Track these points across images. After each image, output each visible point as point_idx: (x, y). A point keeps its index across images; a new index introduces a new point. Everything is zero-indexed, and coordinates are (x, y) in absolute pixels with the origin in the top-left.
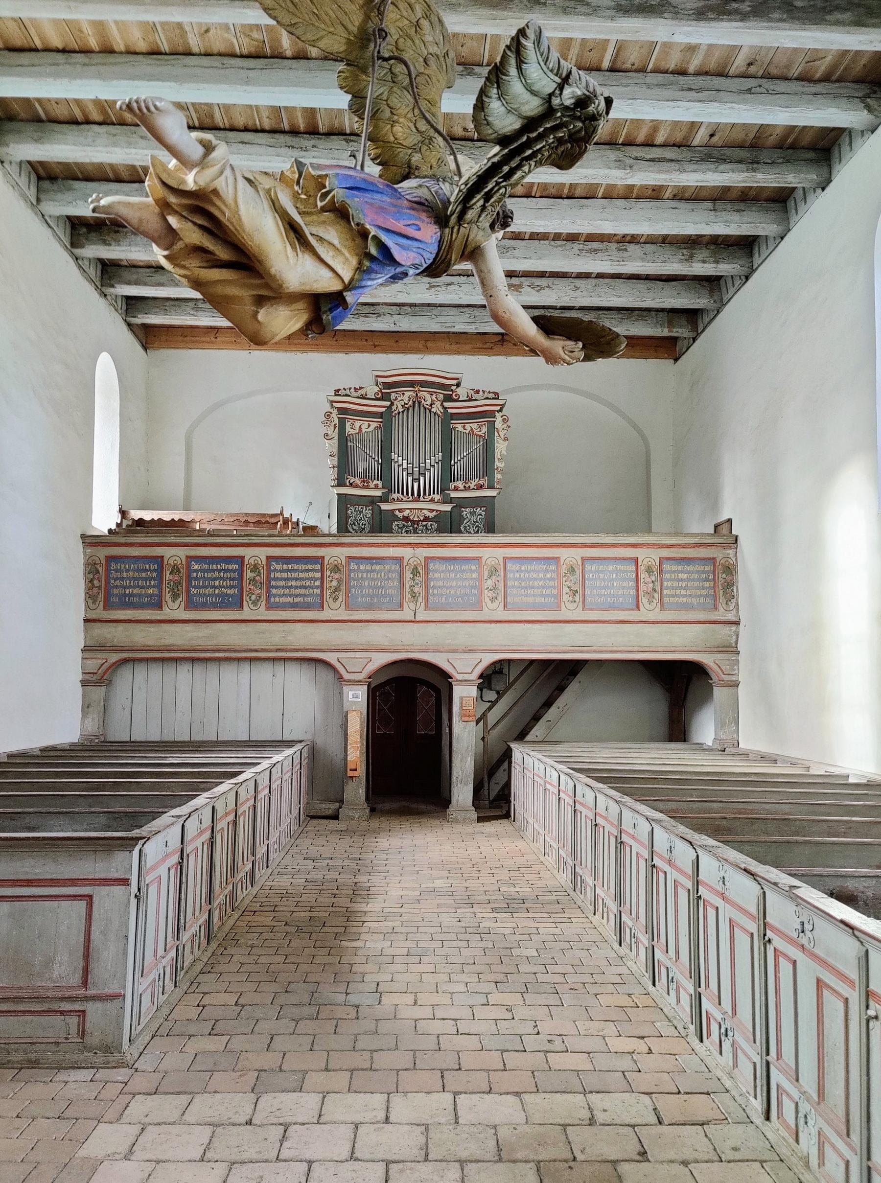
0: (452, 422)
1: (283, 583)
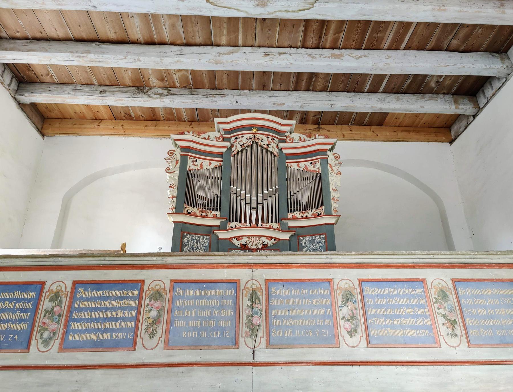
0: (287, 161)
1: (88, 315)
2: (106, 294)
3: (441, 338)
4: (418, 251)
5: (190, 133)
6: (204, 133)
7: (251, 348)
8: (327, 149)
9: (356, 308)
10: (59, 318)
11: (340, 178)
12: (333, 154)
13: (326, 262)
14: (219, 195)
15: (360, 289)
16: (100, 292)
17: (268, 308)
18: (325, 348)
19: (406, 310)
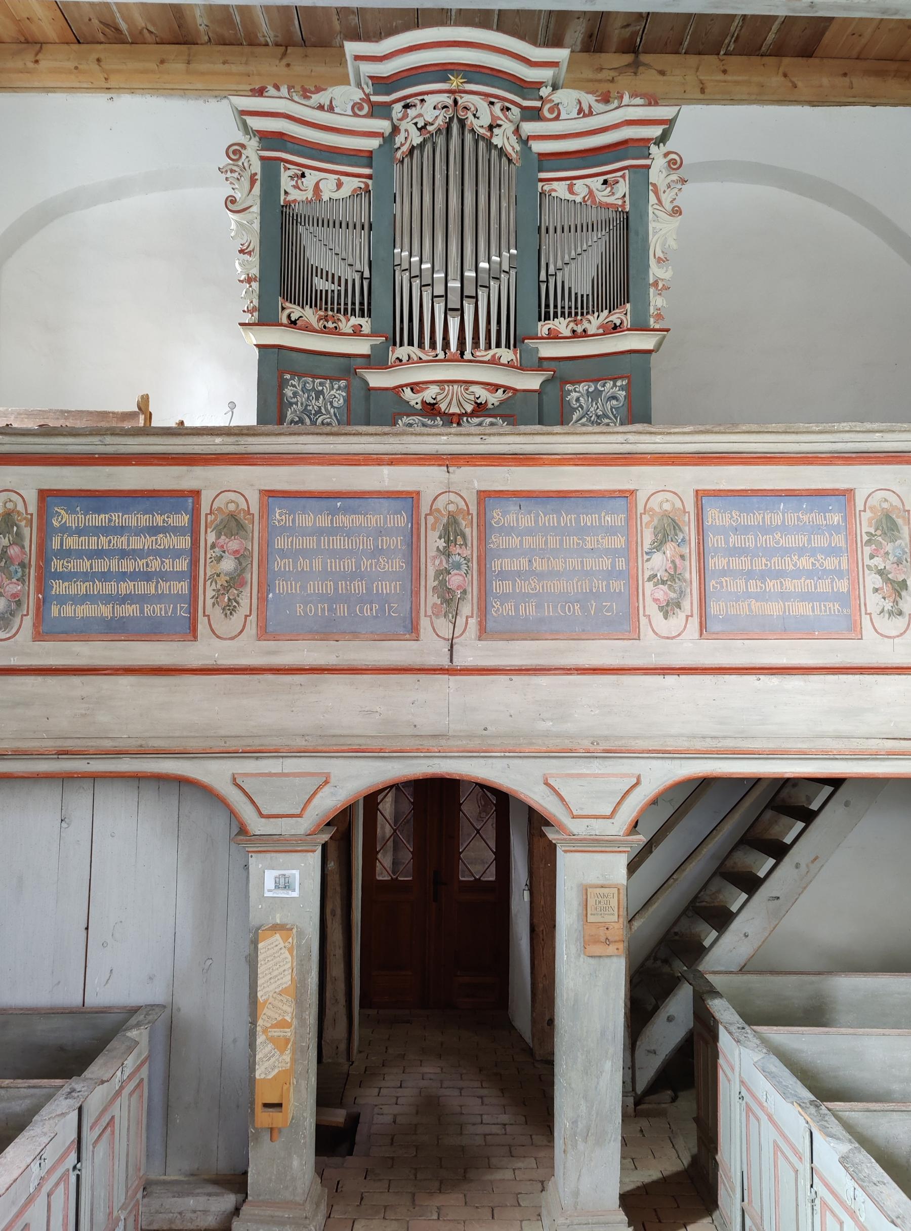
1: (85, 565)
2: (117, 521)
3: (866, 620)
4: (845, 424)
5: (282, 89)
6: (318, 90)
7: (445, 639)
8: (648, 140)
9: (682, 557)
10: (23, 571)
11: (677, 224)
12: (666, 155)
13: (621, 451)
14: (367, 274)
15: (698, 514)
16: (103, 516)
17: (483, 554)
18: (606, 639)
19: (798, 560)
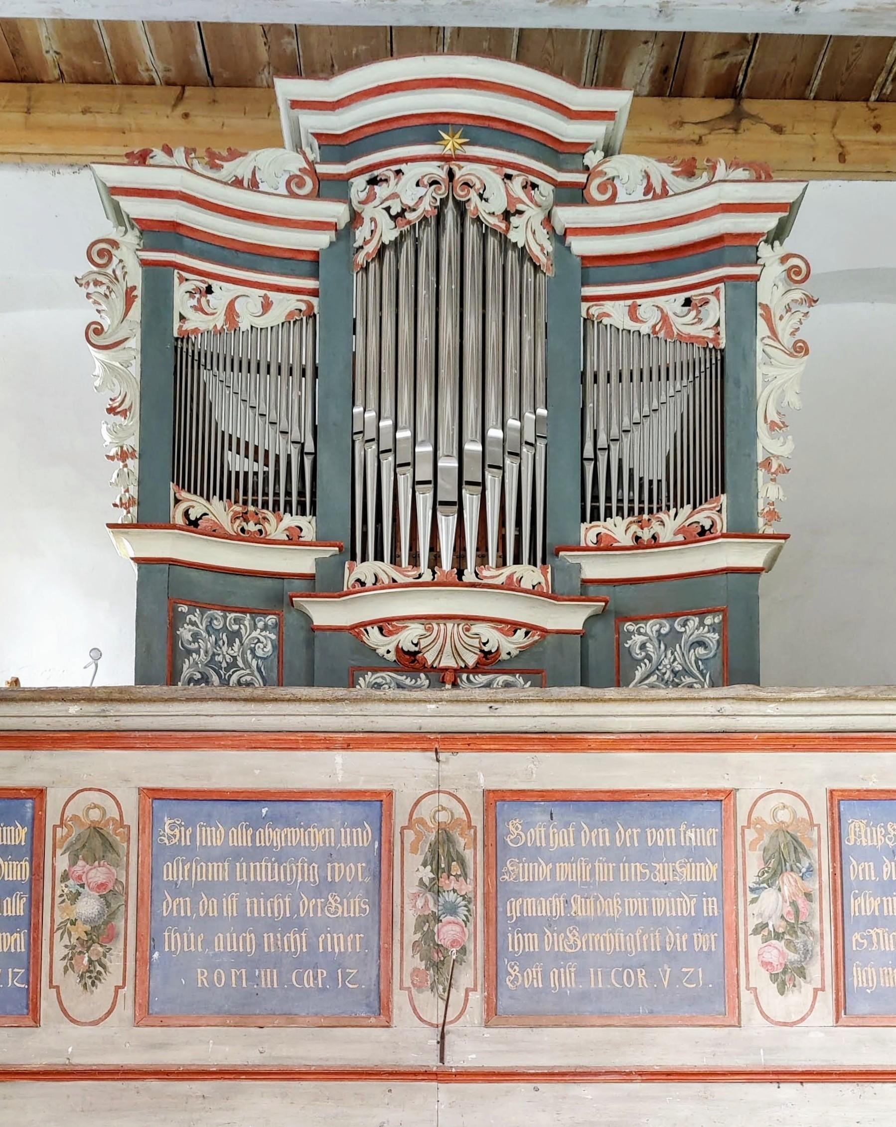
6: (234, 155)
7: (432, 1025)
8: (757, 236)
9: (808, 896)
11: (802, 368)
12: (784, 259)
13: (712, 728)
14: (309, 447)
17: (492, 891)
18: (687, 1026)
